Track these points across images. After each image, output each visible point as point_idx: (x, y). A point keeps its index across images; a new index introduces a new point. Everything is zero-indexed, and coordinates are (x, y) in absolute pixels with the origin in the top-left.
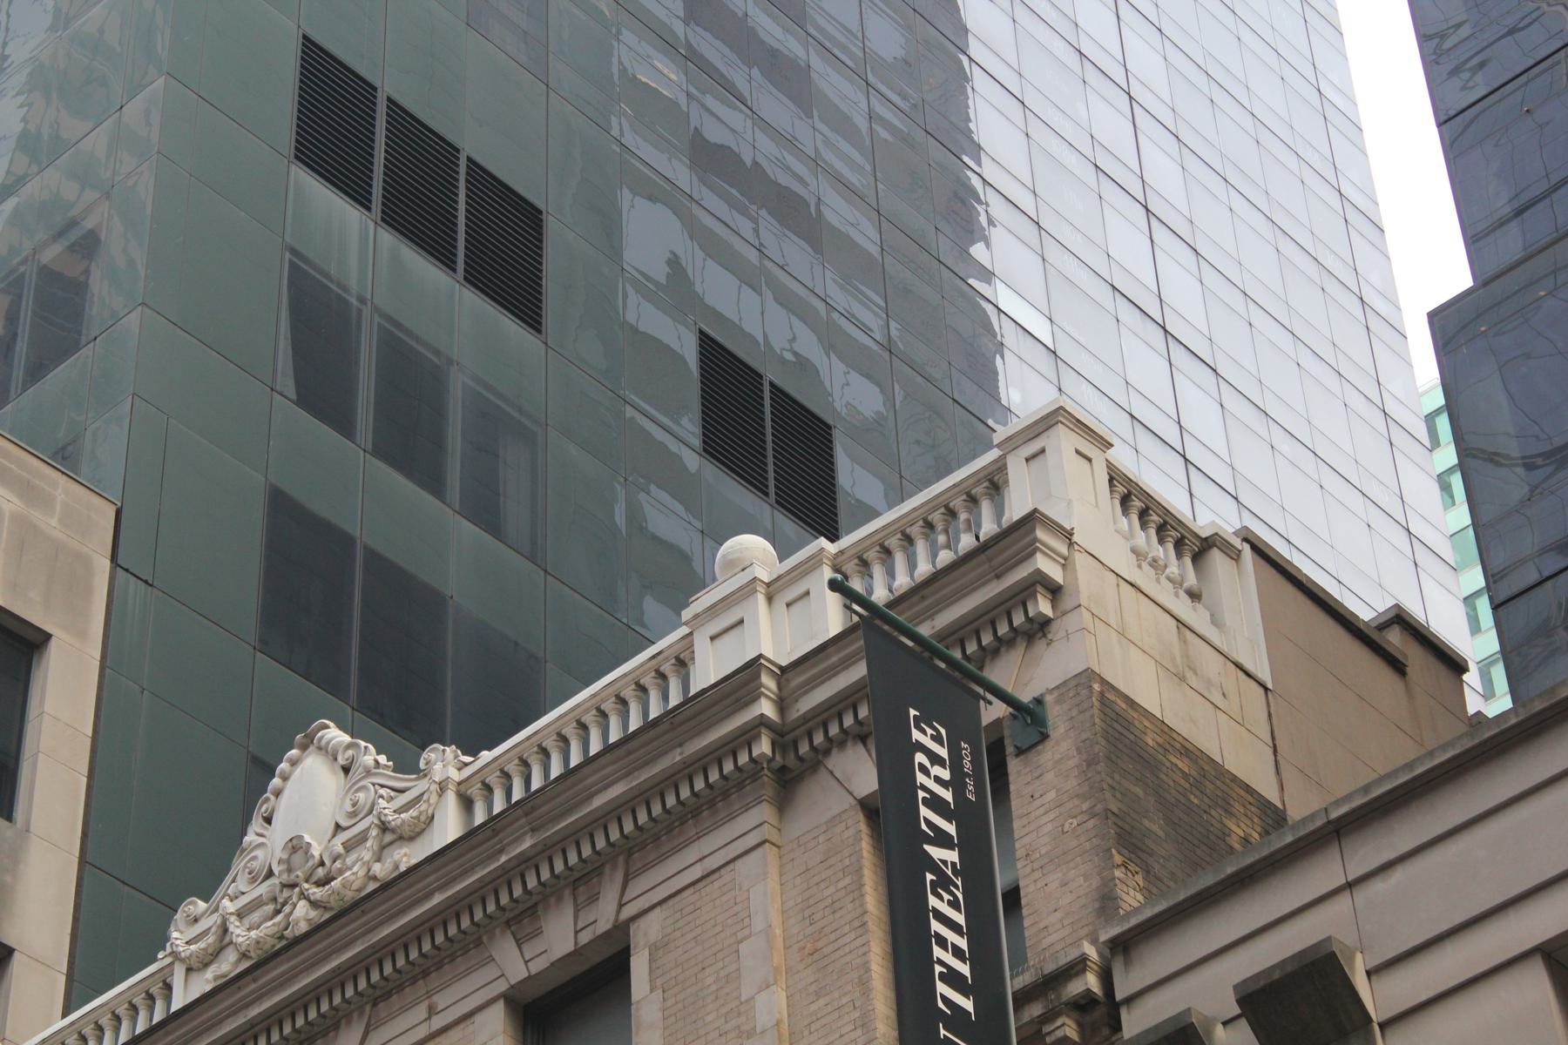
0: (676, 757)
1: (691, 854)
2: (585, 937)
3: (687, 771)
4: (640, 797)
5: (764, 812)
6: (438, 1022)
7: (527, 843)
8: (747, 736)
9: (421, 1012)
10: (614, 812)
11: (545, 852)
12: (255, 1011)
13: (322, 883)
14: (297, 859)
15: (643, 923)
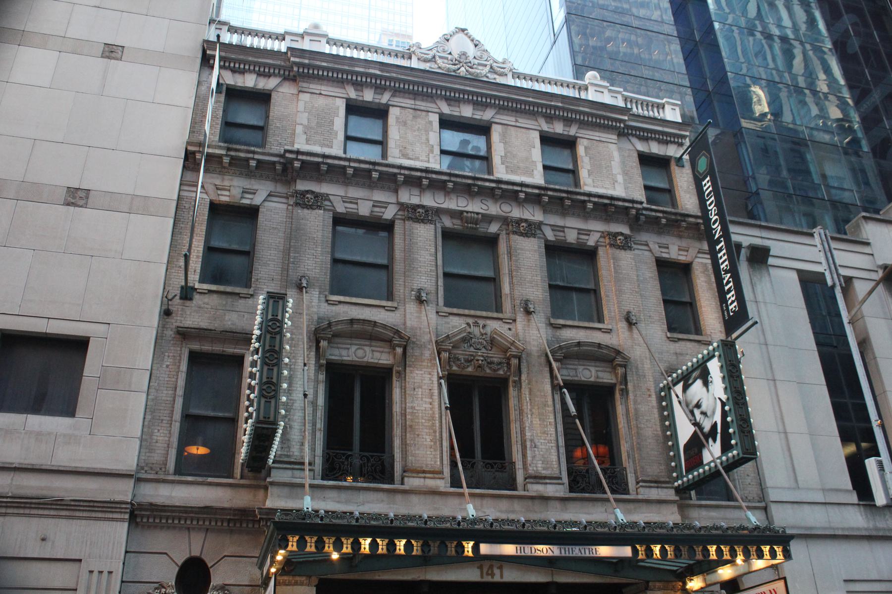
0: (604, 114)
1: (597, 134)
2: (566, 133)
3: (605, 118)
4: (592, 115)
5: (615, 137)
6: (518, 124)
7: (560, 105)
8: (621, 121)
9: (513, 119)
10: (584, 113)
11: (563, 109)
12: (468, 88)
13: (471, 68)
14: (463, 57)
15: (582, 140)
